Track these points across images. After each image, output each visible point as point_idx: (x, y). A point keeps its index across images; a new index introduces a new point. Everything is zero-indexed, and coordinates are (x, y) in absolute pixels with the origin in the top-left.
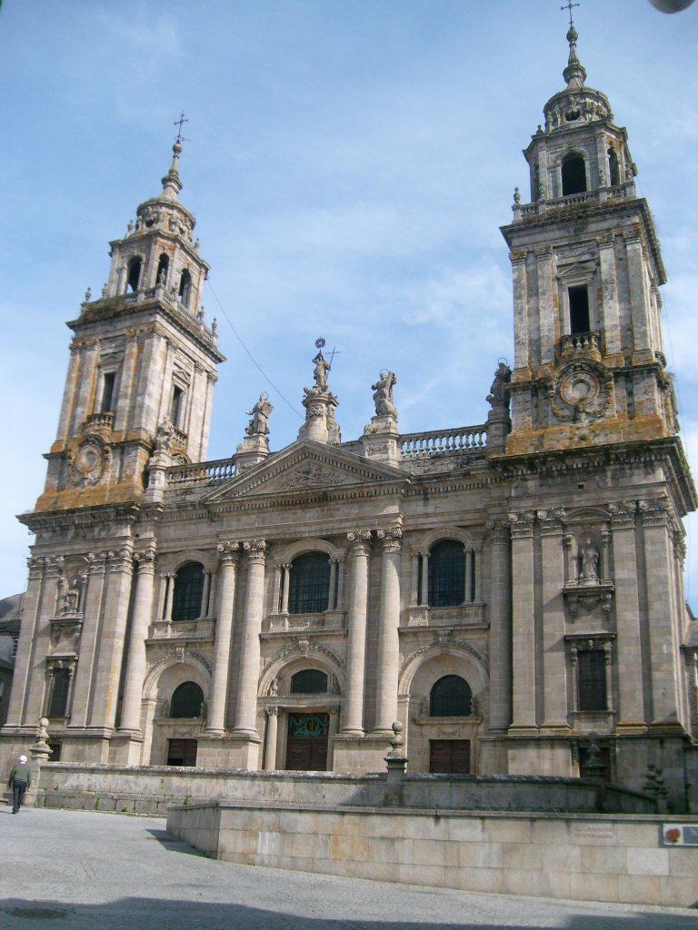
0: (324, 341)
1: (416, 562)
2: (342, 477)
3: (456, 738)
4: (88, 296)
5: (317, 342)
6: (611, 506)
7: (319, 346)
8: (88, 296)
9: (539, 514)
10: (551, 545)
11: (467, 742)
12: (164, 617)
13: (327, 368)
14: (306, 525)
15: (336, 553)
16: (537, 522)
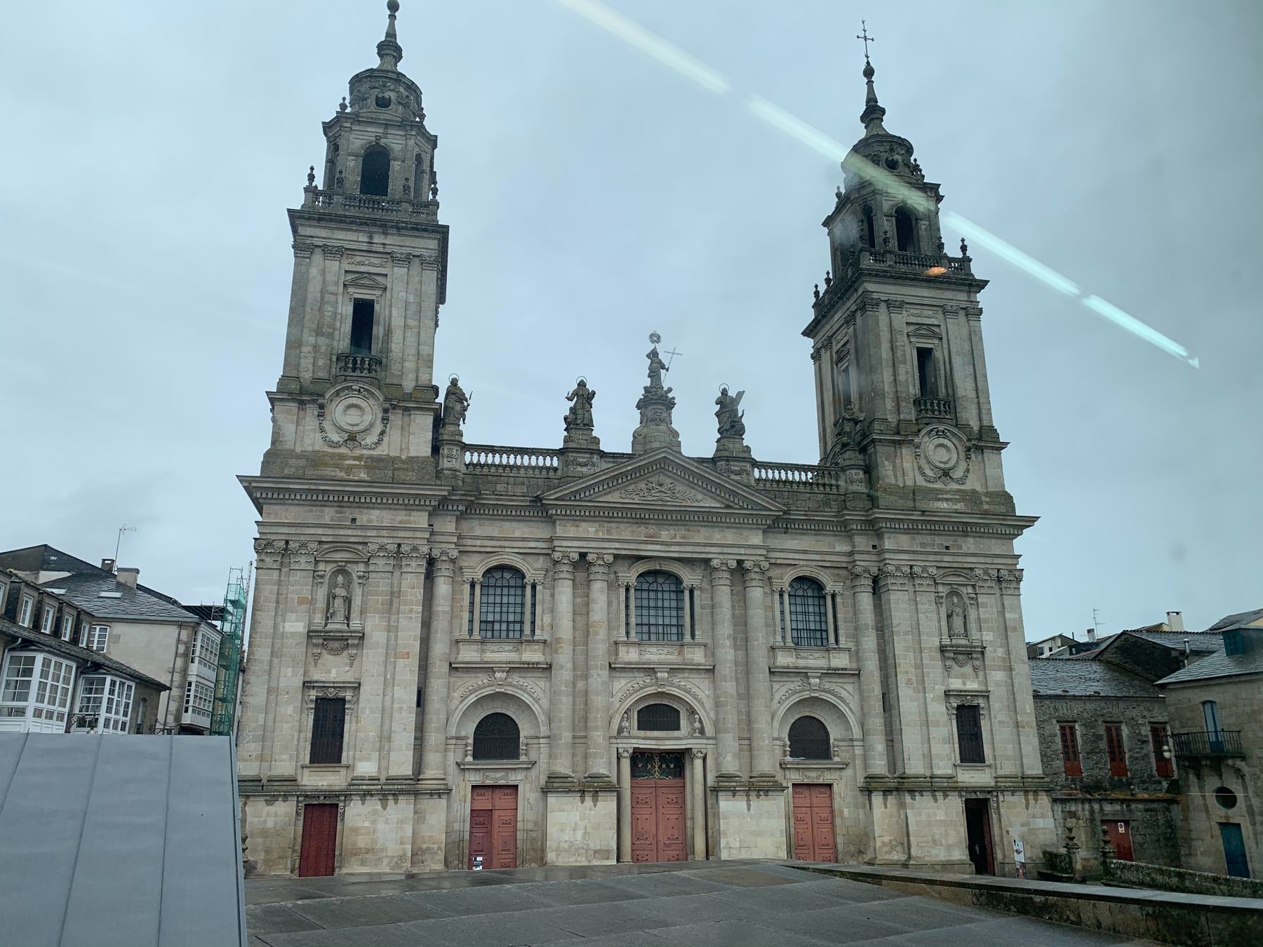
0: (659, 337)
1: (777, 597)
2: (700, 496)
3: (821, 781)
4: (311, 177)
5: (652, 336)
6: (978, 572)
7: (653, 342)
8: (311, 177)
9: (915, 569)
10: (927, 604)
11: (830, 786)
12: (471, 631)
13: (663, 367)
14: (662, 543)
15: (690, 578)
16: (912, 576)
